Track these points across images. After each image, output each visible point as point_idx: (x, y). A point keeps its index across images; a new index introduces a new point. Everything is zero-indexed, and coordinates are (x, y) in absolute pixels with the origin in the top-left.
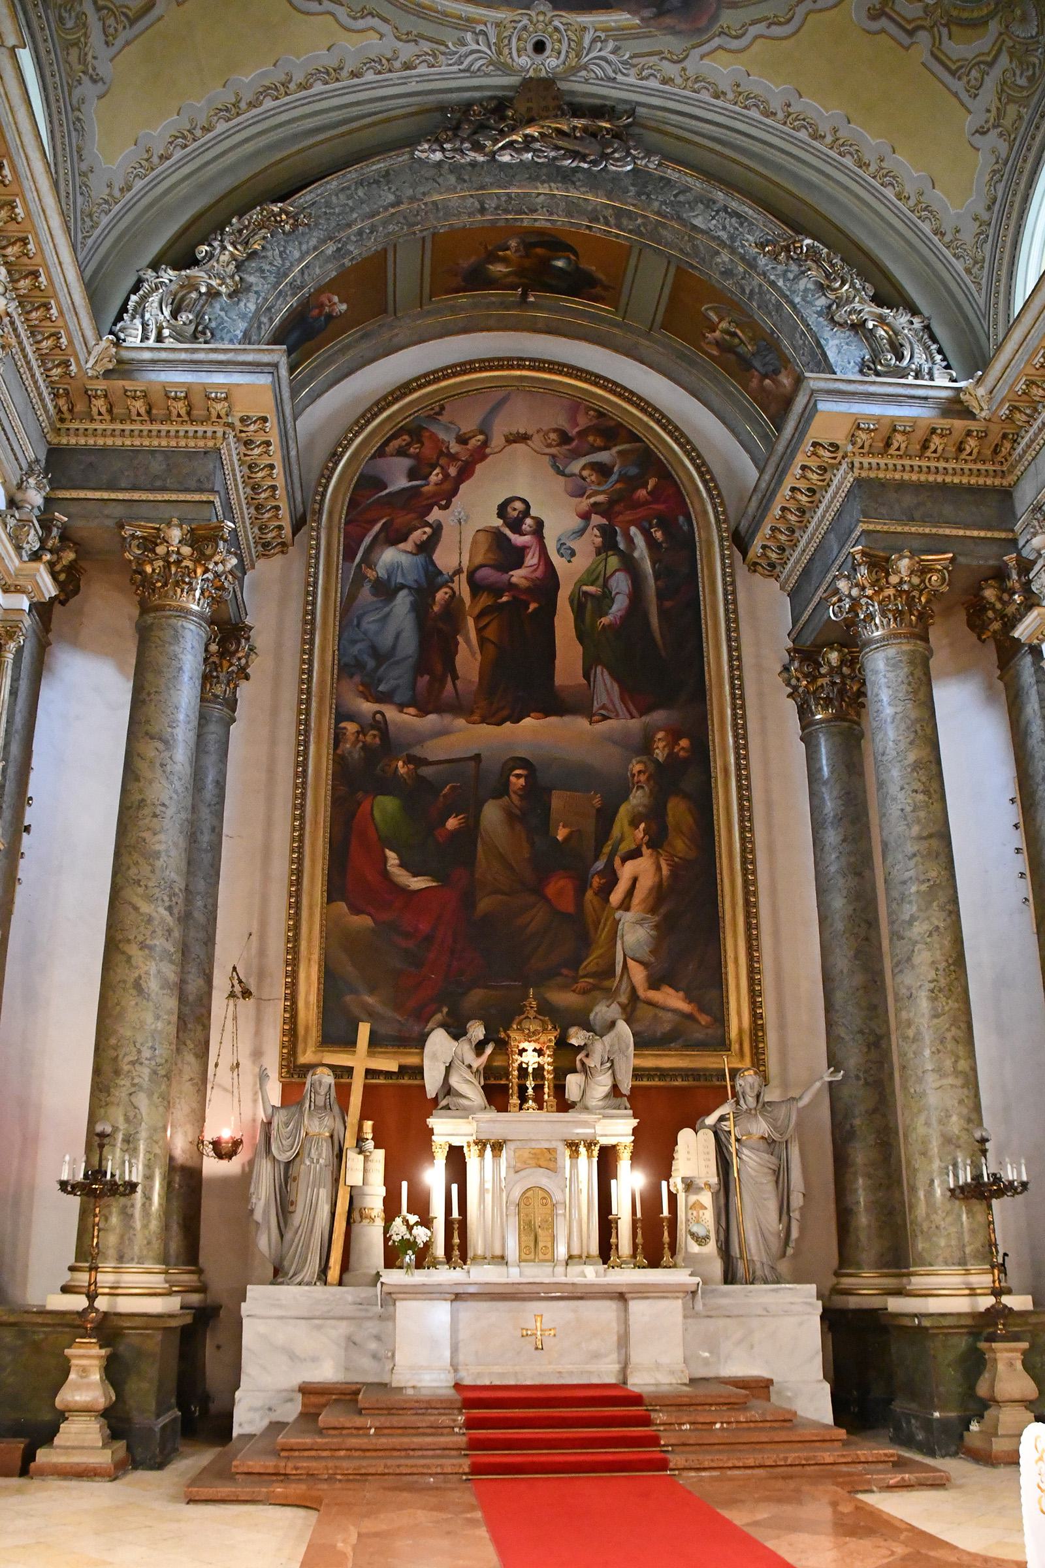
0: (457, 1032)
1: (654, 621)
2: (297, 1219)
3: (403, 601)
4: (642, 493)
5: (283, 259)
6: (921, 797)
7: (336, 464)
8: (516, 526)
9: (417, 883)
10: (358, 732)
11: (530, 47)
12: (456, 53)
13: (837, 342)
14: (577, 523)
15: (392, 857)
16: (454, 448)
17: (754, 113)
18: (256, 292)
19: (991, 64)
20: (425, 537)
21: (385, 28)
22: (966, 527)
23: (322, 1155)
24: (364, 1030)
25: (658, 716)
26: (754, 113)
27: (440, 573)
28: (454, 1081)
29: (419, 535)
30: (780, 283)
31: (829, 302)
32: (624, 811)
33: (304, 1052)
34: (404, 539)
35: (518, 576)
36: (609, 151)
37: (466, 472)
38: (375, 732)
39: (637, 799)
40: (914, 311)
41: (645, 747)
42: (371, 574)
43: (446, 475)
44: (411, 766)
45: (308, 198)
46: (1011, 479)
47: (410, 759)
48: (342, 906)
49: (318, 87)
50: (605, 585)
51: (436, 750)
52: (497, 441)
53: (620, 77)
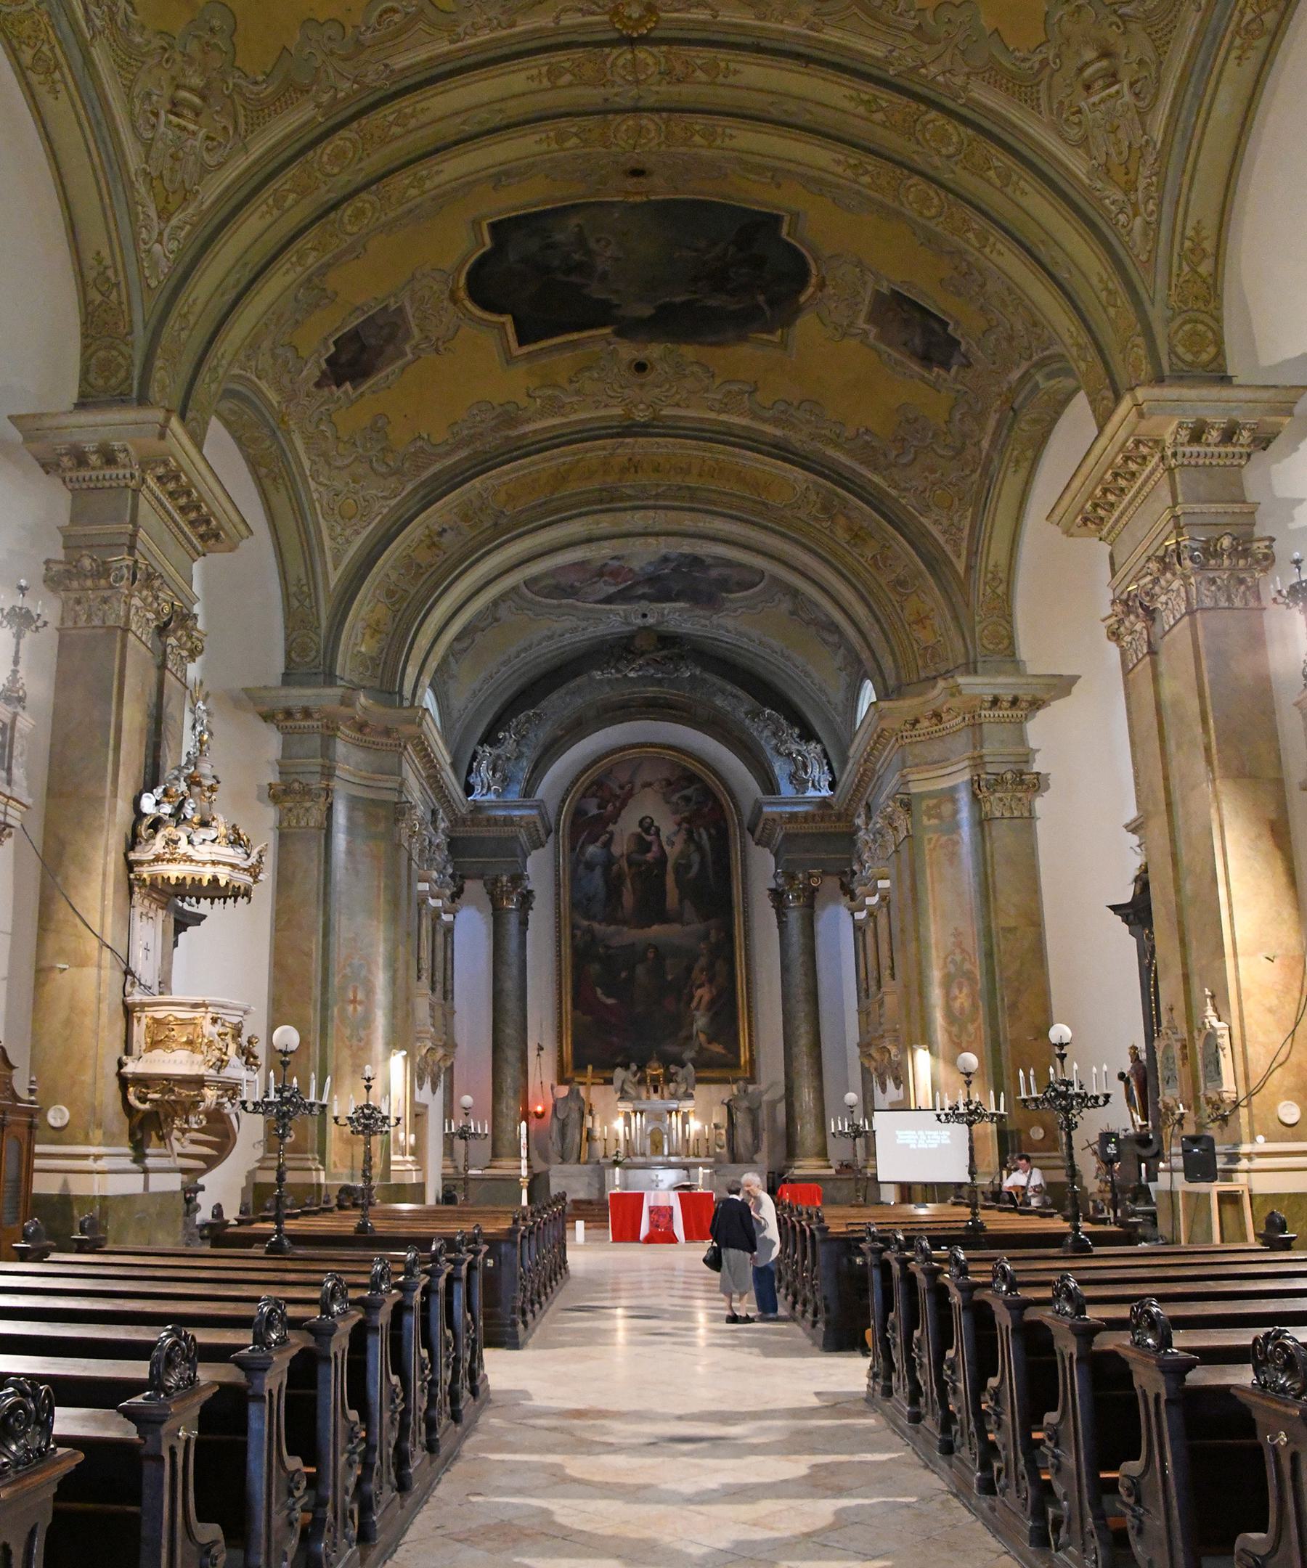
9: (610, 1001)
14: (676, 828)
15: (599, 991)
16: (618, 792)
21: (574, 619)
23: (575, 1115)
24: (590, 1068)
29: (604, 838)
34: (596, 840)
35: (649, 856)
37: (624, 804)
39: (702, 961)
40: (819, 741)
41: (706, 936)
51: (615, 942)
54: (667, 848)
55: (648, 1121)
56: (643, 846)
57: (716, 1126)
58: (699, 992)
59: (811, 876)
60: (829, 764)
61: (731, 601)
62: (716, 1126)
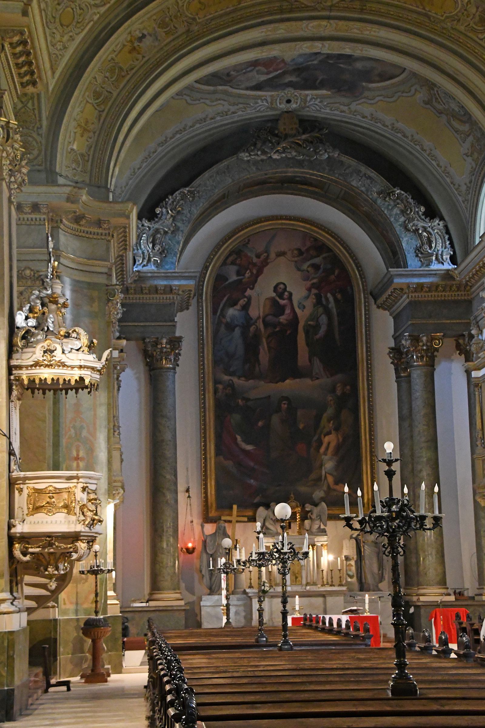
1: (337, 337)
3: (237, 332)
4: (332, 277)
5: (191, 214)
6: (425, 427)
7: (207, 271)
8: (281, 296)
9: (249, 447)
10: (223, 389)
11: (284, 102)
12: (253, 107)
13: (407, 239)
15: (239, 438)
16: (255, 260)
17: (379, 125)
18: (182, 231)
19: (468, 136)
20: (245, 303)
21: (225, 103)
22: (451, 319)
24: (235, 507)
25: (339, 376)
26: (379, 125)
27: (251, 319)
29: (242, 302)
30: (386, 212)
31: (405, 219)
32: (325, 416)
33: (211, 512)
35: (283, 319)
36: (318, 151)
37: (260, 272)
38: (229, 388)
39: (330, 411)
40: (442, 219)
41: (333, 390)
42: (224, 320)
43: (252, 273)
44: (244, 402)
45: (198, 182)
46: (473, 296)
47: (244, 399)
48: (221, 458)
49: (198, 125)
50: (317, 321)
51: (253, 395)
52: (273, 255)
53: (322, 110)
54: (297, 310)
56: (278, 309)
57: (347, 558)
58: (326, 440)
59: (433, 339)
60: (450, 239)
61: (369, 89)
62: (347, 558)
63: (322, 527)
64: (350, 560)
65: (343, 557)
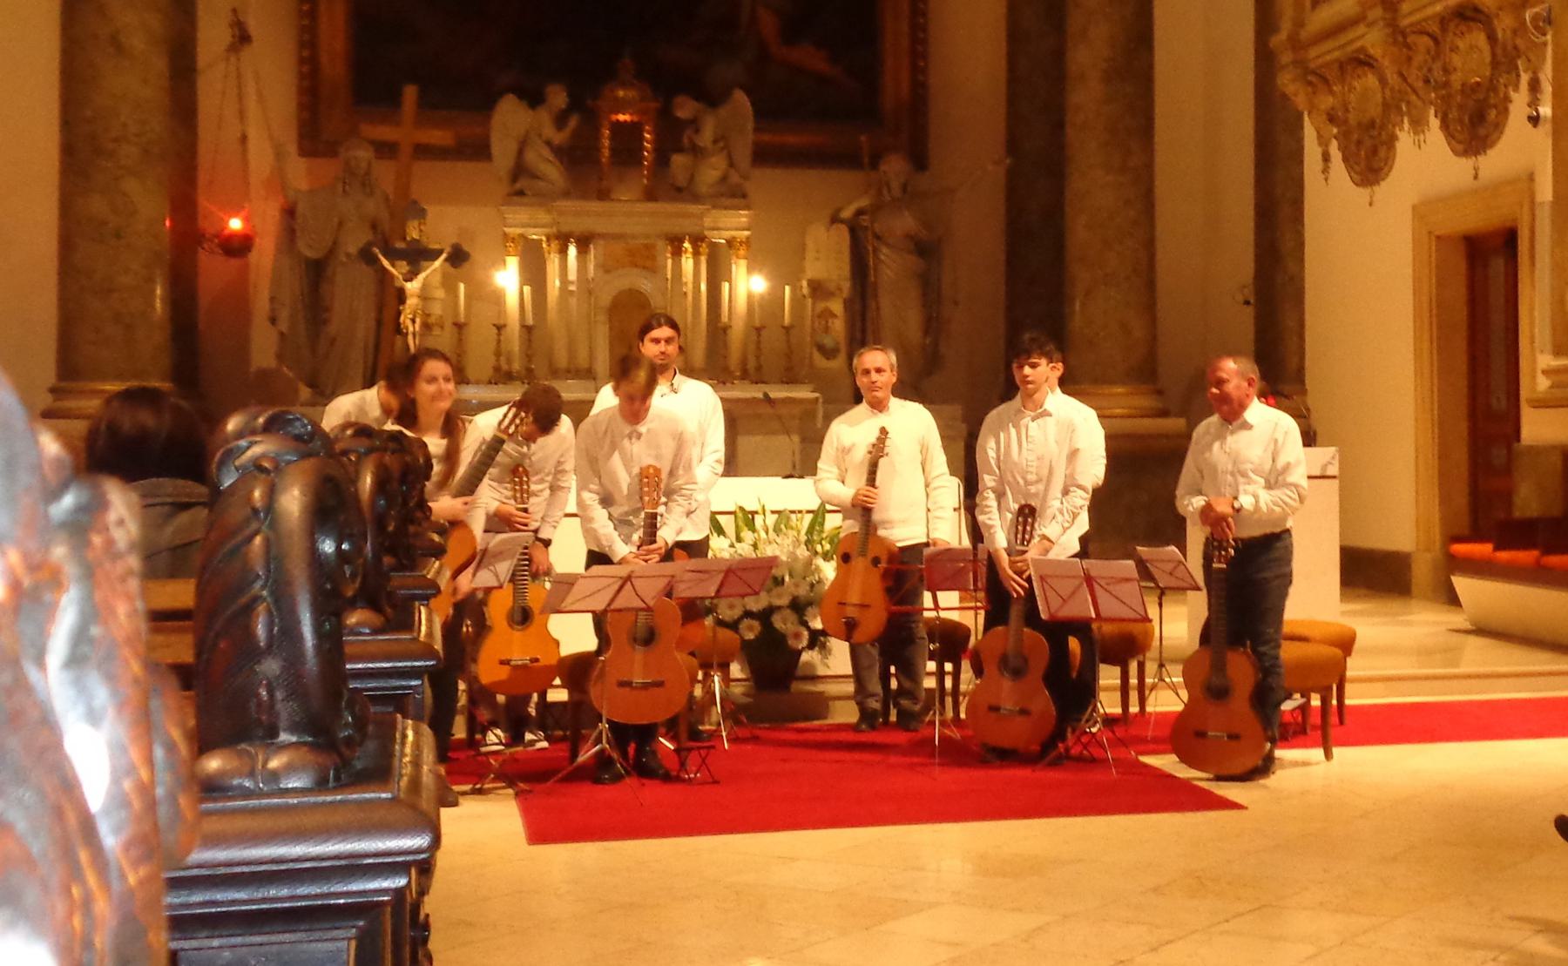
0: (534, 99)
2: (333, 328)
24: (410, 93)
28: (531, 157)
55: (605, 268)
57: (818, 289)
62: (818, 289)
63: (735, 178)
64: (829, 295)
65: (805, 283)
